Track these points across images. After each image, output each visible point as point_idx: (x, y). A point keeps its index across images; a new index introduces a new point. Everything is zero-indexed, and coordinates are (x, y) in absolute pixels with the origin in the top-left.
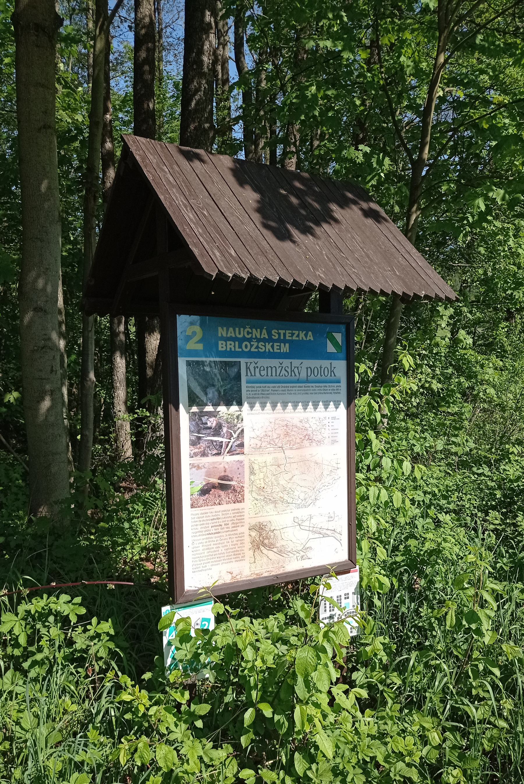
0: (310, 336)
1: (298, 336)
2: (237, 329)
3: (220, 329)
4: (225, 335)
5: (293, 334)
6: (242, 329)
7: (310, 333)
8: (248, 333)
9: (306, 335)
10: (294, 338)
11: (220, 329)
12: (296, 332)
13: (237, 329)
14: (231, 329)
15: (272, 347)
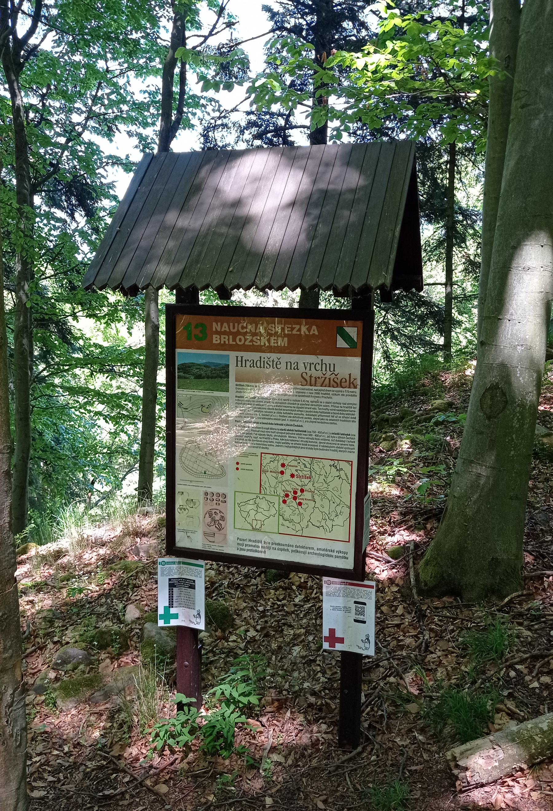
0: (314, 331)
1: (299, 330)
2: (231, 324)
3: (214, 324)
4: (219, 329)
5: (293, 329)
6: (236, 325)
7: (314, 327)
8: (243, 328)
9: (309, 330)
10: (294, 332)
11: (214, 324)
12: (297, 327)
13: (231, 324)
14: (225, 324)
15: (269, 341)
